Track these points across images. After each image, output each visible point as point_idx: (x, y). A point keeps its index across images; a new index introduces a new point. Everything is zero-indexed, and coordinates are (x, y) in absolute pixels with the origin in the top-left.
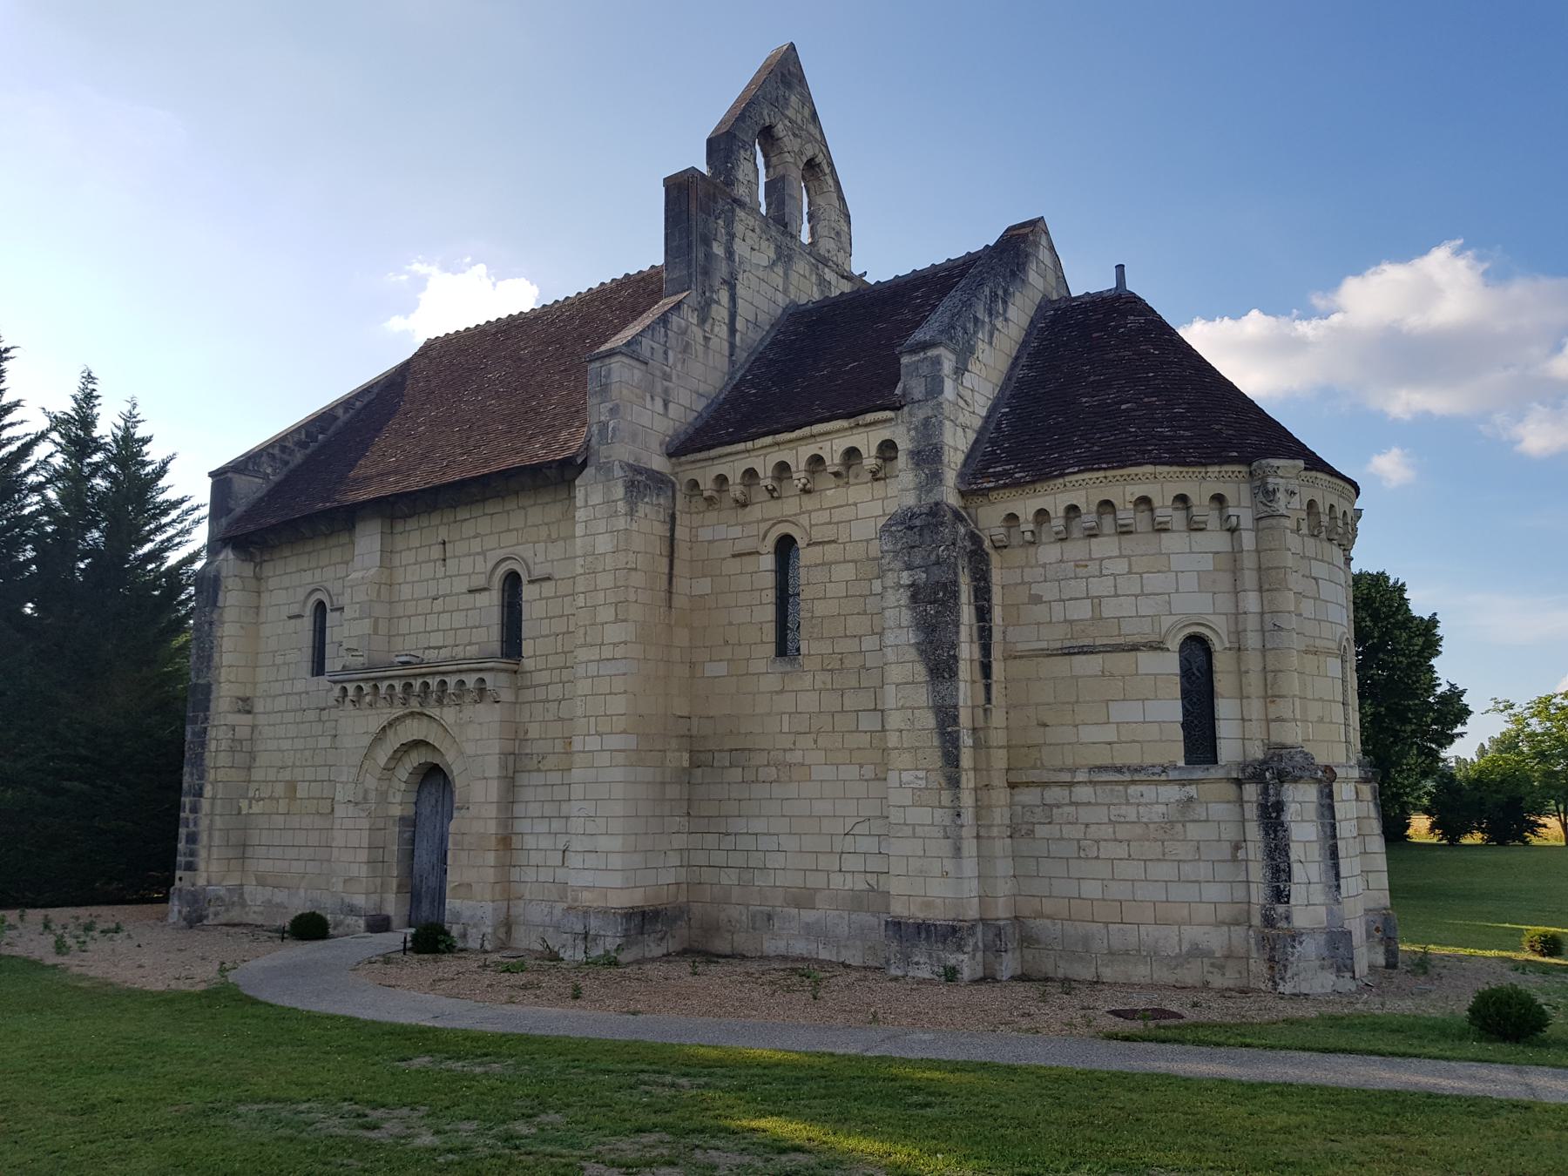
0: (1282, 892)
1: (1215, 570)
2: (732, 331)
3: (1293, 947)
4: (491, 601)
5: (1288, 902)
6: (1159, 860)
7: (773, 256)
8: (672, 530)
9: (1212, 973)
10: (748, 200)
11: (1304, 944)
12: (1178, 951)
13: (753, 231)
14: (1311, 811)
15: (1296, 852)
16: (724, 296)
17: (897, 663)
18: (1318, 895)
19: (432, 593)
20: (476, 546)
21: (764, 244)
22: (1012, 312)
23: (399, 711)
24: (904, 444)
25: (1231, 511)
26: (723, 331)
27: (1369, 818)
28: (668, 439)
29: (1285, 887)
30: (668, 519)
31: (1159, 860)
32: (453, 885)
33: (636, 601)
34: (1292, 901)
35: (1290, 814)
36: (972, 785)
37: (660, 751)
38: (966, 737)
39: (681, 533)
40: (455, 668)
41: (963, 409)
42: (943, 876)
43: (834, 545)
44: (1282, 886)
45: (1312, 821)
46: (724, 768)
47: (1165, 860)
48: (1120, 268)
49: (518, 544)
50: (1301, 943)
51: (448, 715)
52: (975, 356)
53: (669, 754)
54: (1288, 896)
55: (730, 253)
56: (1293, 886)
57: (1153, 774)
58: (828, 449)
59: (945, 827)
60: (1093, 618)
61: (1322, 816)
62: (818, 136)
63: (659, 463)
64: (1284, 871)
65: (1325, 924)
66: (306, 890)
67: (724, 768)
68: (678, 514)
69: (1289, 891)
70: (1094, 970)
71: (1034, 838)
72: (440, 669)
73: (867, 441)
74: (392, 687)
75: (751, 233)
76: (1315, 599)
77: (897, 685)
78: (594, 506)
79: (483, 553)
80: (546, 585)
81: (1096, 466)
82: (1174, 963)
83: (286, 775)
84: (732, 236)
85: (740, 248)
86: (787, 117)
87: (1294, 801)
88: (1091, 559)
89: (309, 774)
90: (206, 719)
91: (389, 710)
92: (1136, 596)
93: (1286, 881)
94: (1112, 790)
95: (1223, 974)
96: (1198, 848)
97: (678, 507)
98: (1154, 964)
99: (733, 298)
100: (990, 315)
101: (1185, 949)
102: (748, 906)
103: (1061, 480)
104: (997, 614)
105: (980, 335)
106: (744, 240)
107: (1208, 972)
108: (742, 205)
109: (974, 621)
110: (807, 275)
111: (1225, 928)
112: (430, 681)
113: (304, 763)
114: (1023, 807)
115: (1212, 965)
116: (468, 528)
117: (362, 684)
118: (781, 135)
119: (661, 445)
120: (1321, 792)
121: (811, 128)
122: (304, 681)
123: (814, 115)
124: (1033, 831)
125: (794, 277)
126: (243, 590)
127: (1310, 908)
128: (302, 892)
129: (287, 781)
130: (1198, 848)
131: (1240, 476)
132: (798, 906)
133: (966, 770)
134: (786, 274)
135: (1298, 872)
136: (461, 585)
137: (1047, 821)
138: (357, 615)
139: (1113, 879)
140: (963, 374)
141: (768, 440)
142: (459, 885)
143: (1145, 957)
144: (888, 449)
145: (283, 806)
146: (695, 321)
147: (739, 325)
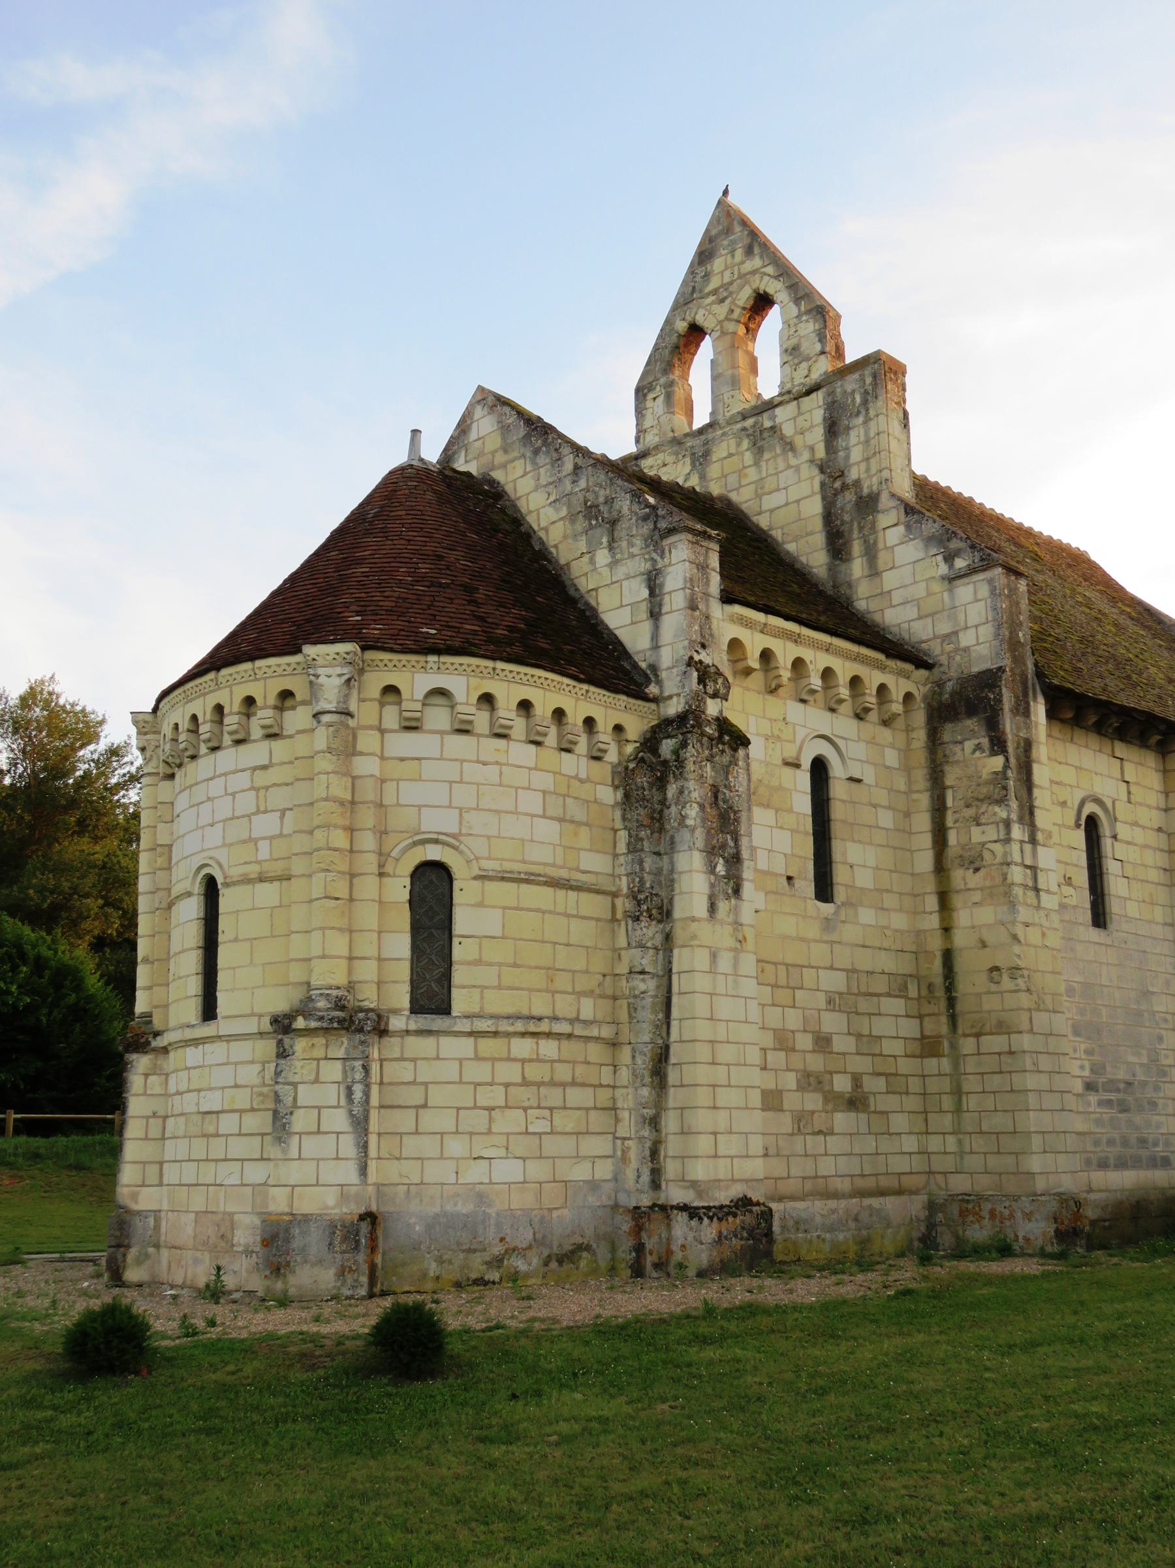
7: (688, 468)
13: (665, 465)
48: (415, 433)
75: (665, 469)
86: (708, 294)
110: (733, 450)
125: (714, 470)
134: (703, 477)
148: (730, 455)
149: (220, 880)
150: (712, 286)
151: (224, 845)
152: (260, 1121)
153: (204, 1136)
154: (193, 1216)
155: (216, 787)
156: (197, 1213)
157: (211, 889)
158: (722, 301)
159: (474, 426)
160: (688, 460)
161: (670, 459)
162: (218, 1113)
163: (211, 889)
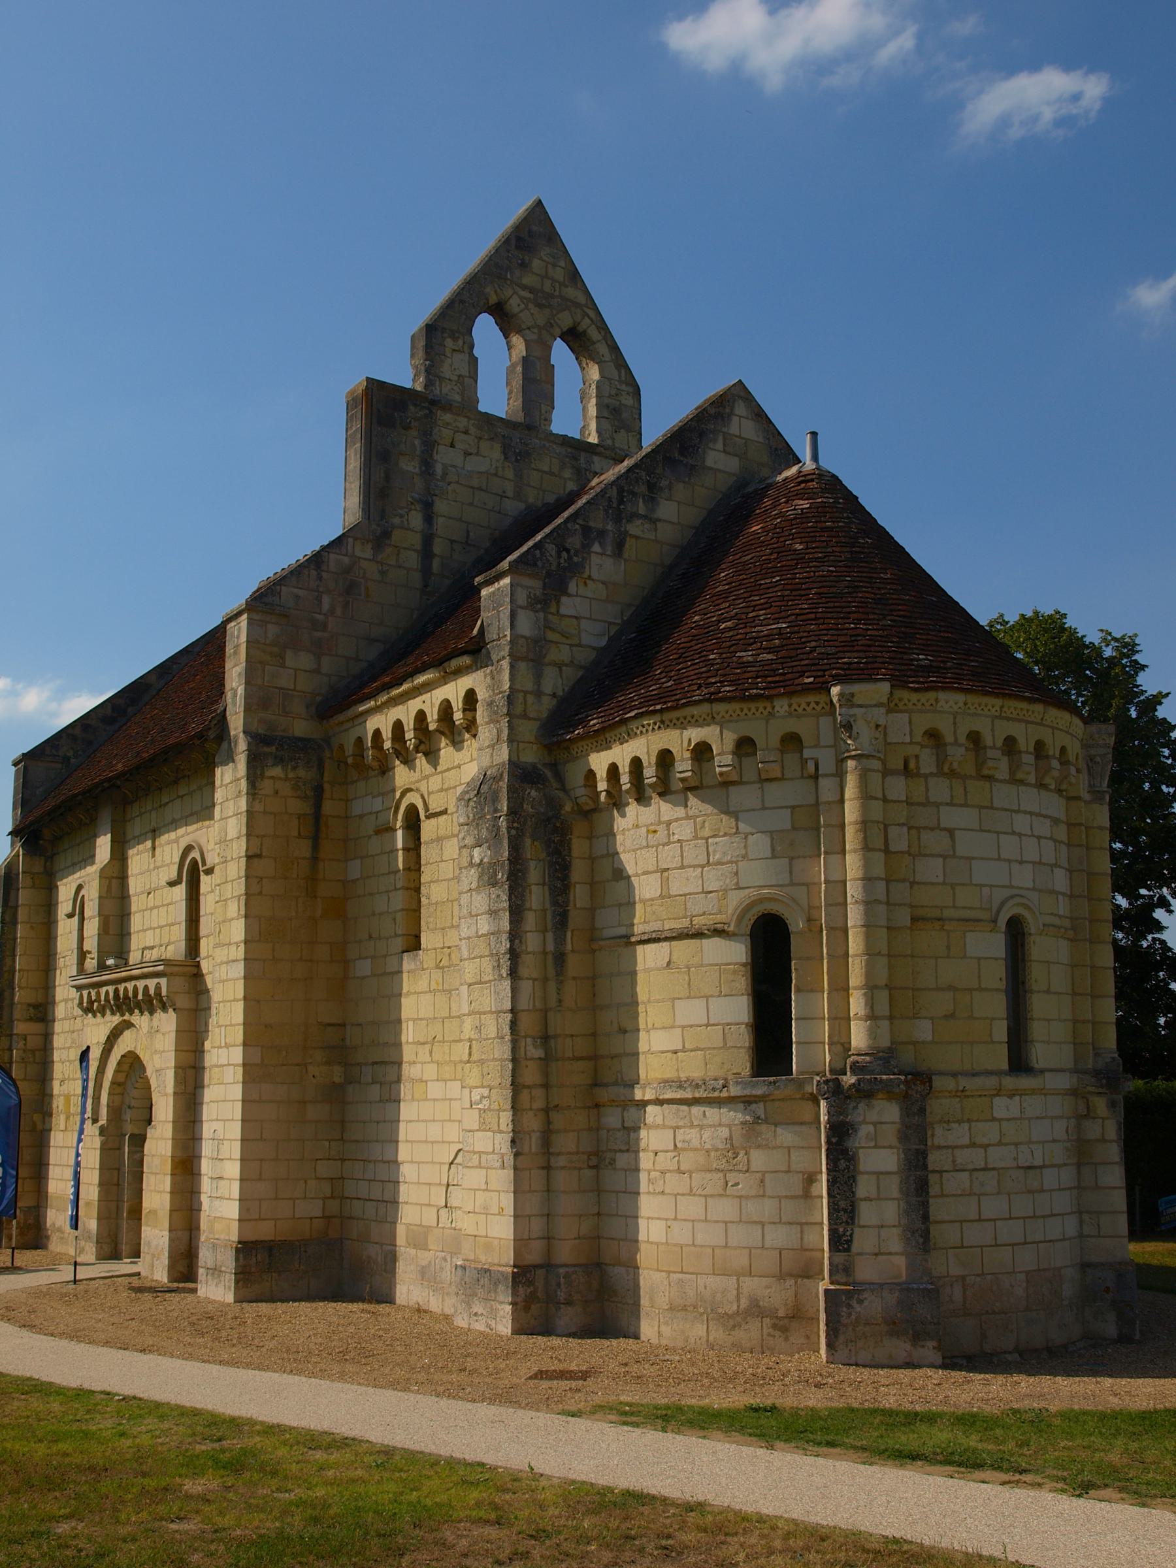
0: (840, 1237)
1: (794, 828)
2: (426, 553)
3: (849, 1306)
5: (848, 1250)
6: (721, 1195)
8: (318, 805)
9: (774, 1336)
10: (458, 398)
11: (866, 1303)
12: (735, 1308)
13: (466, 432)
14: (890, 1134)
15: (864, 1187)
16: (416, 520)
17: (469, 959)
18: (894, 1241)
21: (484, 445)
22: (667, 510)
23: (116, 1019)
24: (481, 695)
25: (807, 753)
26: (412, 560)
27: (1103, 1140)
28: (319, 699)
29: (845, 1231)
30: (310, 793)
31: (721, 1195)
33: (260, 893)
34: (855, 1247)
35: (861, 1139)
36: (539, 1104)
37: (298, 1065)
38: (530, 1048)
39: (328, 807)
41: (556, 643)
42: (499, 1214)
43: (445, 817)
44: (841, 1230)
45: (891, 1147)
46: (368, 1084)
47: (726, 1196)
50: (860, 1302)
52: (586, 575)
53: (312, 1069)
54: (849, 1242)
55: (427, 464)
56: (856, 1230)
57: (714, 1089)
58: (428, 702)
59: (503, 1156)
60: (662, 897)
61: (903, 1137)
62: (581, 299)
63: (301, 728)
64: (845, 1210)
65: (904, 1278)
67: (368, 1084)
68: (327, 786)
69: (851, 1235)
70: (656, 1328)
71: (615, 1169)
73: (453, 691)
74: (107, 993)
75: (463, 436)
76: (944, 857)
77: (470, 985)
78: (226, 785)
81: (658, 707)
82: (731, 1322)
84: (430, 446)
85: (444, 457)
87: (864, 1122)
88: (660, 823)
92: (703, 867)
93: (847, 1223)
94: (678, 1110)
95: (787, 1339)
96: (762, 1181)
97: (326, 779)
98: (711, 1323)
99: (429, 519)
100: (618, 518)
101: (744, 1303)
102: (382, 1245)
103: (624, 728)
104: (579, 895)
105: (596, 548)
106: (452, 446)
107: (769, 1335)
108: (447, 407)
109: (548, 905)
111: (790, 1282)
114: (608, 1131)
115: (774, 1326)
118: (516, 310)
119: (307, 707)
120: (906, 1112)
121: (570, 292)
123: (574, 276)
124: (614, 1160)
126: (33, 887)
127: (880, 1257)
130: (762, 1181)
131: (819, 708)
132: (416, 1247)
133: (529, 1087)
135: (867, 1214)
137: (625, 1148)
139: (676, 1219)
140: (558, 602)
141: (383, 698)
143: (702, 1314)
144: (470, 698)
146: (368, 554)
147: (438, 548)
148: (552, 474)
149: (1032, 925)
150: (528, 280)
151: (1034, 889)
152: (1067, 1176)
153: (1029, 1192)
154: (1022, 1277)
155: (1021, 823)
156: (1027, 1273)
157: (1016, 932)
158: (540, 306)
159: (735, 419)
160: (498, 447)
161: (473, 430)
162: (1041, 1167)
163: (1016, 932)
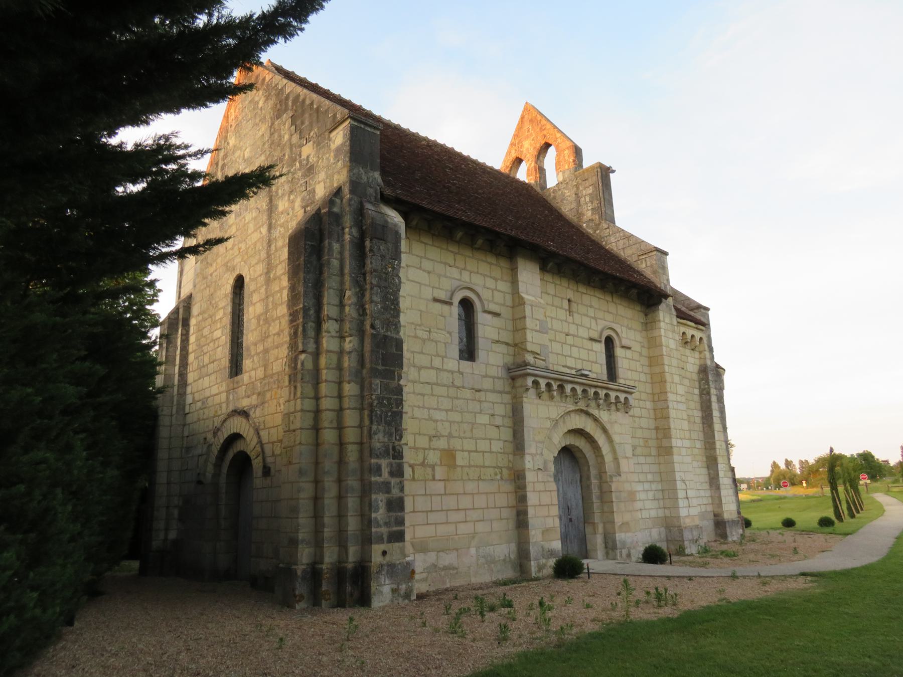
4: (601, 348)
19: (567, 331)
20: (591, 312)
32: (619, 524)
40: (618, 387)
49: (613, 322)
51: (604, 416)
66: (478, 548)
72: (610, 386)
79: (595, 319)
80: (628, 351)
83: (442, 444)
89: (469, 445)
90: (400, 378)
91: (565, 405)
112: (599, 391)
113: (462, 435)
116: (586, 299)
117: (552, 382)
122: (453, 362)
128: (473, 551)
129: (444, 450)
136: (583, 333)
138: (538, 328)
142: (622, 524)
145: (440, 472)
